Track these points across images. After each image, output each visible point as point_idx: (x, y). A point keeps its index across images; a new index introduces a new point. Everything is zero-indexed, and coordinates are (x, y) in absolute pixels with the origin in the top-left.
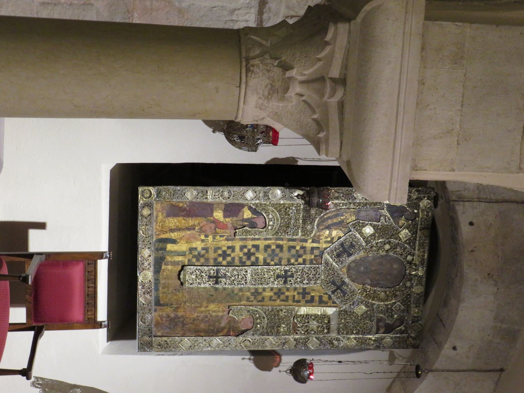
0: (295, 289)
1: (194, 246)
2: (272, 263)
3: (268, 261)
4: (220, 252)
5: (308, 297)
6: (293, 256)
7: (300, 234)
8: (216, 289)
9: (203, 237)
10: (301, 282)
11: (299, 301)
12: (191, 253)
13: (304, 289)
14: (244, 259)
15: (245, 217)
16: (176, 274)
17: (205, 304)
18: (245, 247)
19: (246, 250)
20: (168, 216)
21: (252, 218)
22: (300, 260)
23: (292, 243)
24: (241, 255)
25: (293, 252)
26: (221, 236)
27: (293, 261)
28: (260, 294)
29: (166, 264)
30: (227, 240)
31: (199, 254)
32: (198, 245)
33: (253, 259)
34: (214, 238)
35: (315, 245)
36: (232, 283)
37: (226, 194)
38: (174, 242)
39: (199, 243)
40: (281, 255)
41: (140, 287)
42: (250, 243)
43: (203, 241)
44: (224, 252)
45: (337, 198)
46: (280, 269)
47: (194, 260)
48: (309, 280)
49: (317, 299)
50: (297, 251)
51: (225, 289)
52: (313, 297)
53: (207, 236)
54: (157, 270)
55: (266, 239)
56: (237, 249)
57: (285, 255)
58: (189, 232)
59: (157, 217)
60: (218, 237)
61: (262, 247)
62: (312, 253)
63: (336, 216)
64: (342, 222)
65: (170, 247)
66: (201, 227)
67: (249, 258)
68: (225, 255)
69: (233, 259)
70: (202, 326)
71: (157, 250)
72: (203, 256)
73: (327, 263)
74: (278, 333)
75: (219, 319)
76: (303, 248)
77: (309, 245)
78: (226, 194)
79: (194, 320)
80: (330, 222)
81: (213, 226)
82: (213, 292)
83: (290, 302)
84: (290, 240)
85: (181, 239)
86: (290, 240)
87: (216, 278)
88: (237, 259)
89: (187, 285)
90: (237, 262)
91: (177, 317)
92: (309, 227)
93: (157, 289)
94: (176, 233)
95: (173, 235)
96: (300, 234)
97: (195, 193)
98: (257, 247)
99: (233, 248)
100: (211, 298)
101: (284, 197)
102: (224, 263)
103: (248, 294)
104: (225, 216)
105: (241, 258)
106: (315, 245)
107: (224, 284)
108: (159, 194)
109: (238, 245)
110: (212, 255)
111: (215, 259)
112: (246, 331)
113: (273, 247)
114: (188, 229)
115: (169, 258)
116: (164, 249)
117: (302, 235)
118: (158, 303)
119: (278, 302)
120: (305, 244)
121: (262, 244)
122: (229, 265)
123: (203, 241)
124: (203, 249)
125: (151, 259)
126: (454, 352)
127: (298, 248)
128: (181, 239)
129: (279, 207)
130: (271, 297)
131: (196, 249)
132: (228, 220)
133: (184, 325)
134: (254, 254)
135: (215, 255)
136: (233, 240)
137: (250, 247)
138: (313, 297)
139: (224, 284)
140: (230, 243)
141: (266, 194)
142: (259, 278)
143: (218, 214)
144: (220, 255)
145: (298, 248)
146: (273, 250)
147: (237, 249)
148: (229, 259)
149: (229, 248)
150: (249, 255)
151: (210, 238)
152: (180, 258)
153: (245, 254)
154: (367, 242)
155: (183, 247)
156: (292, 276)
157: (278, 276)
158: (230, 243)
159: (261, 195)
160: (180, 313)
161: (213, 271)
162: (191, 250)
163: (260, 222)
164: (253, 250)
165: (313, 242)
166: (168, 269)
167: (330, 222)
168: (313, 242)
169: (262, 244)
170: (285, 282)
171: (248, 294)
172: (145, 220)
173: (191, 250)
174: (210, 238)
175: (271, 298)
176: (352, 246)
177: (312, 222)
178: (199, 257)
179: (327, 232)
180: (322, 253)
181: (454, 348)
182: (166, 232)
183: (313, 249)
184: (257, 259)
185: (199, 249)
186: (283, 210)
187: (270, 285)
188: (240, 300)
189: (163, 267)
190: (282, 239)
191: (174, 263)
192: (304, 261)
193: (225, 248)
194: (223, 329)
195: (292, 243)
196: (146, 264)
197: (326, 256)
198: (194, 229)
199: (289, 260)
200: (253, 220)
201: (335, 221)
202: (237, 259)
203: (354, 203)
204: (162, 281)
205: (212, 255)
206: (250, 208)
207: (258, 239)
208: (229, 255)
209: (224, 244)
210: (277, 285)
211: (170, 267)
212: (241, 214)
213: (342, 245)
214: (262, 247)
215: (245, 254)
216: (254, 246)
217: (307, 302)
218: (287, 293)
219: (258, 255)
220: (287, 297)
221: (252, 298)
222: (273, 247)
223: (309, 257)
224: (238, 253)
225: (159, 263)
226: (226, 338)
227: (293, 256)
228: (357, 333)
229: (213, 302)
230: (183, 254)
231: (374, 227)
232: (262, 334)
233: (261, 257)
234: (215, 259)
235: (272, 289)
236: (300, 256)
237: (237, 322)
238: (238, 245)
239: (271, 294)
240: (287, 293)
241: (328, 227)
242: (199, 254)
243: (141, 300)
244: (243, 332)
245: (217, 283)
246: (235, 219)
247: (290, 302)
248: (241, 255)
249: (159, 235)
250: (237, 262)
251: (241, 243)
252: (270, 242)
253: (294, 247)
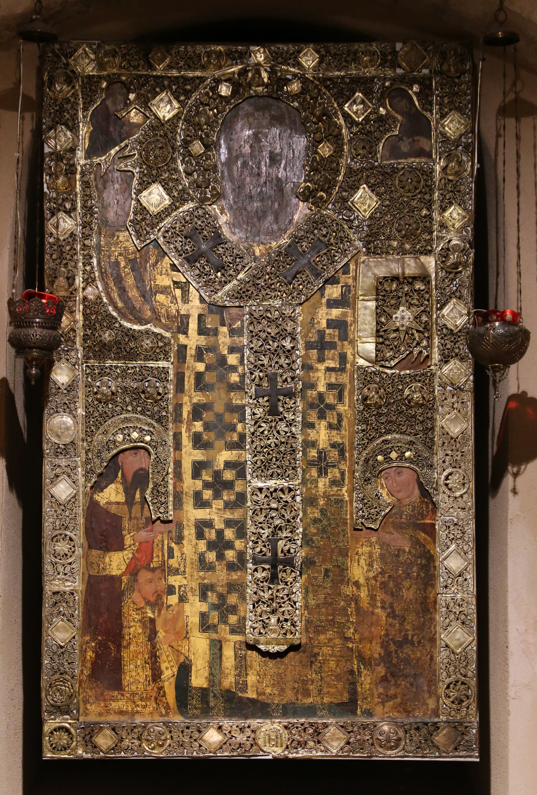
1: (195, 620)
2: (239, 427)
3: (235, 437)
4: (211, 556)
9: (173, 600)
10: (289, 353)
12: (213, 628)
15: (121, 498)
18: (198, 495)
20: (118, 685)
21: (124, 482)
23: (189, 382)
24: (218, 504)
25: (210, 378)
26: (171, 555)
30: (180, 539)
31: (215, 607)
33: (228, 475)
34: (176, 572)
35: (193, 325)
37: (62, 547)
39: (187, 607)
43: (182, 599)
44: (211, 546)
47: (233, 619)
48: (282, 335)
50: (208, 368)
53: (171, 590)
56: (202, 514)
58: (161, 634)
59: (121, 712)
60: (173, 563)
61: (199, 455)
64: (132, 262)
66: (148, 603)
67: (229, 485)
72: (222, 597)
76: (199, 356)
80: (133, 293)
81: (144, 576)
88: (228, 515)
94: (163, 666)
96: (162, 364)
104: (121, 548)
105: (228, 505)
106: (193, 325)
112: (421, 485)
114: (152, 635)
115: (229, 681)
117: (167, 359)
124: (203, 597)
127: (201, 367)
130: (330, 426)
131: (203, 616)
132: (128, 541)
136: (180, 526)
137: (199, 484)
143: (114, 565)
144: (220, 557)
145: (201, 367)
146: (207, 427)
147: (202, 514)
148: (229, 534)
149: (200, 535)
151: (175, 581)
152: (228, 653)
153: (217, 495)
156: (272, 379)
157: (273, 411)
158: (189, 532)
159: (63, 462)
165: (185, 333)
167: (133, 293)
172: (126, 742)
174: (175, 581)
182: (161, 688)
183: (201, 331)
184: (228, 465)
185: (204, 607)
189: (251, 694)
190: (179, 407)
193: (202, 546)
194: (416, 542)
196: (241, 738)
198: (152, 621)
200: (130, 477)
202: (228, 515)
204: (290, 696)
206: (98, 487)
208: (220, 533)
212: (113, 509)
214: (199, 455)
215: (217, 495)
220: (330, 386)
226: (442, 534)
234: (231, 567)
236: (223, 360)
242: (215, 607)
245: (289, 562)
246: (126, 524)
248: (218, 504)
249: (167, 707)
252: (185, 435)
253: (199, 376)
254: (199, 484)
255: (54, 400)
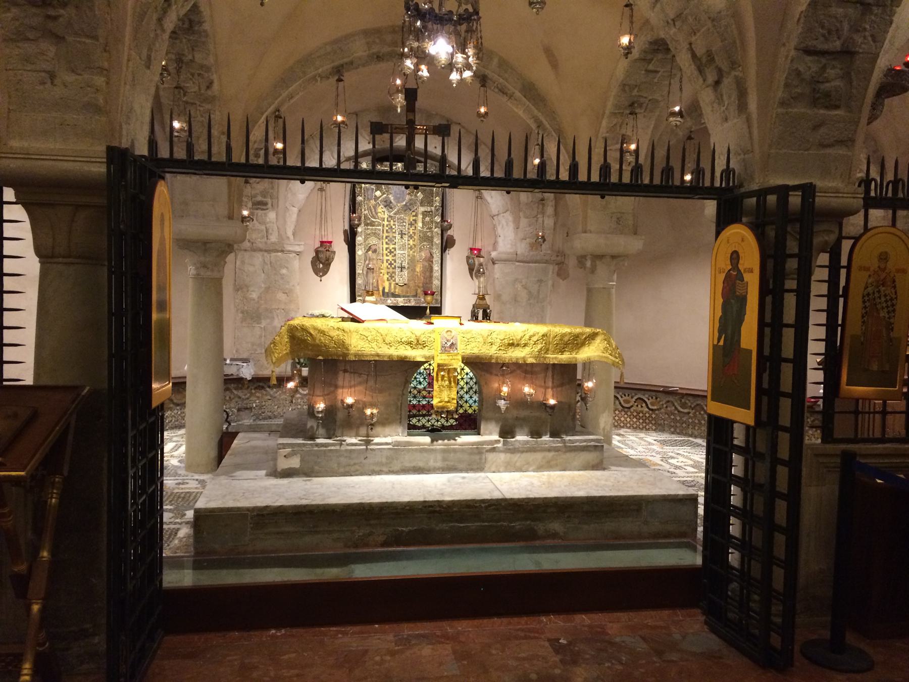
0: (408, 229)
4: (389, 266)
5: (413, 222)
6: (392, 231)
7: (379, 228)
8: (408, 268)
9: (382, 275)
10: (405, 226)
11: (415, 227)
13: (409, 224)
14: (392, 254)
16: (401, 288)
17: (416, 273)
19: (389, 254)
22: (394, 227)
23: (385, 231)
24: (391, 256)
25: (389, 230)
27: (394, 231)
28: (411, 247)
29: (395, 292)
30: (383, 263)
32: (386, 276)
33: (393, 250)
35: (386, 220)
36: (405, 260)
37: (359, 264)
38: (384, 288)
40: (391, 237)
41: (406, 305)
42: (385, 252)
44: (389, 264)
45: (361, 210)
46: (398, 237)
48: (404, 222)
49: (414, 218)
51: (408, 263)
52: (413, 220)
54: (399, 296)
55: (383, 244)
56: (388, 258)
57: (391, 235)
61: (387, 246)
62: (390, 221)
63: (371, 210)
64: (374, 207)
65: (386, 290)
67: (393, 252)
68: (391, 264)
69: (393, 260)
70: (428, 274)
71: (388, 296)
73: (395, 214)
74: (432, 237)
75: (424, 267)
76: (387, 226)
77: (386, 223)
78: (359, 264)
79: (424, 278)
80: (374, 213)
82: (410, 270)
83: (416, 231)
84: (383, 232)
85: (382, 285)
86: (383, 232)
87: (402, 268)
88: (393, 258)
89: (406, 282)
90: (394, 258)
91: (423, 287)
92: (376, 223)
93: (408, 297)
95: (381, 289)
97: (359, 279)
98: (387, 249)
99: (387, 261)
100: (414, 270)
101: (361, 236)
102: (395, 264)
103: (411, 252)
106: (386, 220)
107: (405, 264)
108: (359, 296)
109: (385, 258)
110: (391, 270)
111: (393, 268)
113: (387, 240)
115: (392, 291)
116: (388, 293)
118: (416, 296)
119: (415, 237)
120: (385, 225)
121: (385, 246)
122: (395, 262)
123: (384, 275)
125: (392, 299)
126: (438, 147)
127: (387, 228)
128: (382, 285)
129: (366, 239)
133: (427, 283)
134: (390, 250)
135: (391, 269)
137: (387, 252)
138: (413, 220)
139: (405, 264)
140: (385, 262)
141: (360, 245)
142: (403, 247)
145: (387, 228)
147: (388, 258)
148: (393, 262)
150: (391, 252)
151: (382, 271)
154: (384, 194)
155: (386, 284)
156: (401, 231)
157: (402, 237)
158: (385, 262)
159: (360, 247)
160: (421, 285)
161: (398, 270)
162: (388, 280)
163: (374, 248)
164: (388, 250)
166: (398, 291)
167: (374, 213)
168: (384, 221)
169: (385, 246)
170: (405, 234)
171: (411, 252)
173: (388, 280)
174: (382, 271)
175: (414, 241)
176: (386, 202)
177: (374, 222)
178: (392, 277)
179: (379, 214)
180: (390, 216)
181: (436, 147)
183: (388, 221)
186: (367, 237)
187: (406, 241)
188: (414, 256)
191: (395, 288)
192: (394, 225)
193: (387, 264)
194: (429, 264)
195: (385, 231)
197: (392, 214)
199: (394, 233)
201: (373, 210)
202: (393, 258)
203: (364, 201)
204: (404, 294)
205: (391, 270)
207: (383, 248)
209: (385, 264)
210: (406, 237)
211: (397, 290)
213: (385, 207)
214: (387, 246)
216: (386, 250)
217: (416, 223)
218: (411, 233)
219: (391, 248)
221: (413, 250)
222: (387, 240)
223: (392, 223)
224: (390, 258)
225: (394, 295)
226: (434, 262)
227: (392, 231)
228: (433, 197)
229: (415, 269)
230: (390, 284)
231: (376, 191)
232: (432, 245)
233: (392, 246)
235: (408, 240)
236: (392, 227)
237: (425, 257)
238: (385, 258)
239: (411, 240)
240: (411, 233)
241: (377, 213)
243: (413, 304)
244: (431, 255)
245: (404, 268)
247: (416, 231)
248: (391, 256)
250: (394, 258)
251: (385, 256)
253: (387, 230)
254: (387, 252)
255: (358, 234)
